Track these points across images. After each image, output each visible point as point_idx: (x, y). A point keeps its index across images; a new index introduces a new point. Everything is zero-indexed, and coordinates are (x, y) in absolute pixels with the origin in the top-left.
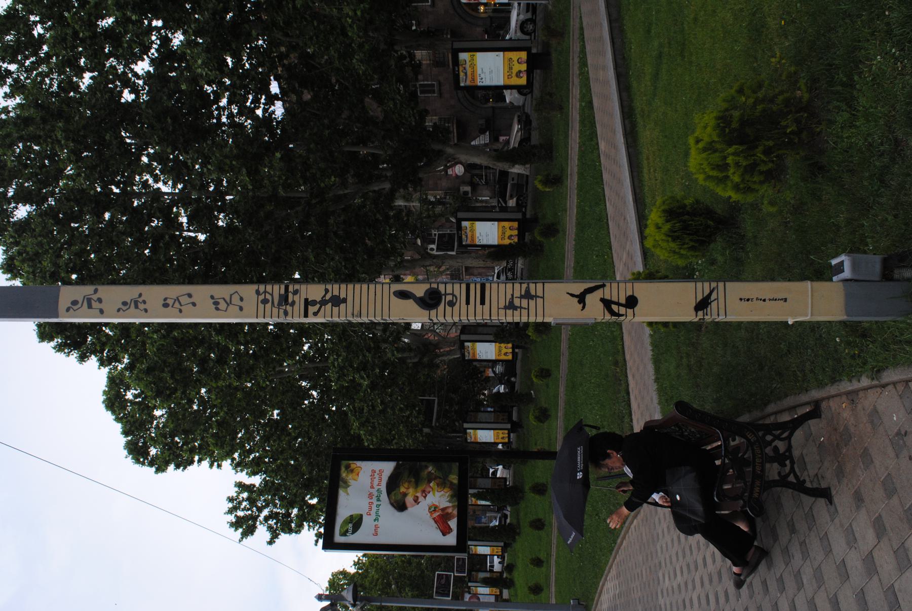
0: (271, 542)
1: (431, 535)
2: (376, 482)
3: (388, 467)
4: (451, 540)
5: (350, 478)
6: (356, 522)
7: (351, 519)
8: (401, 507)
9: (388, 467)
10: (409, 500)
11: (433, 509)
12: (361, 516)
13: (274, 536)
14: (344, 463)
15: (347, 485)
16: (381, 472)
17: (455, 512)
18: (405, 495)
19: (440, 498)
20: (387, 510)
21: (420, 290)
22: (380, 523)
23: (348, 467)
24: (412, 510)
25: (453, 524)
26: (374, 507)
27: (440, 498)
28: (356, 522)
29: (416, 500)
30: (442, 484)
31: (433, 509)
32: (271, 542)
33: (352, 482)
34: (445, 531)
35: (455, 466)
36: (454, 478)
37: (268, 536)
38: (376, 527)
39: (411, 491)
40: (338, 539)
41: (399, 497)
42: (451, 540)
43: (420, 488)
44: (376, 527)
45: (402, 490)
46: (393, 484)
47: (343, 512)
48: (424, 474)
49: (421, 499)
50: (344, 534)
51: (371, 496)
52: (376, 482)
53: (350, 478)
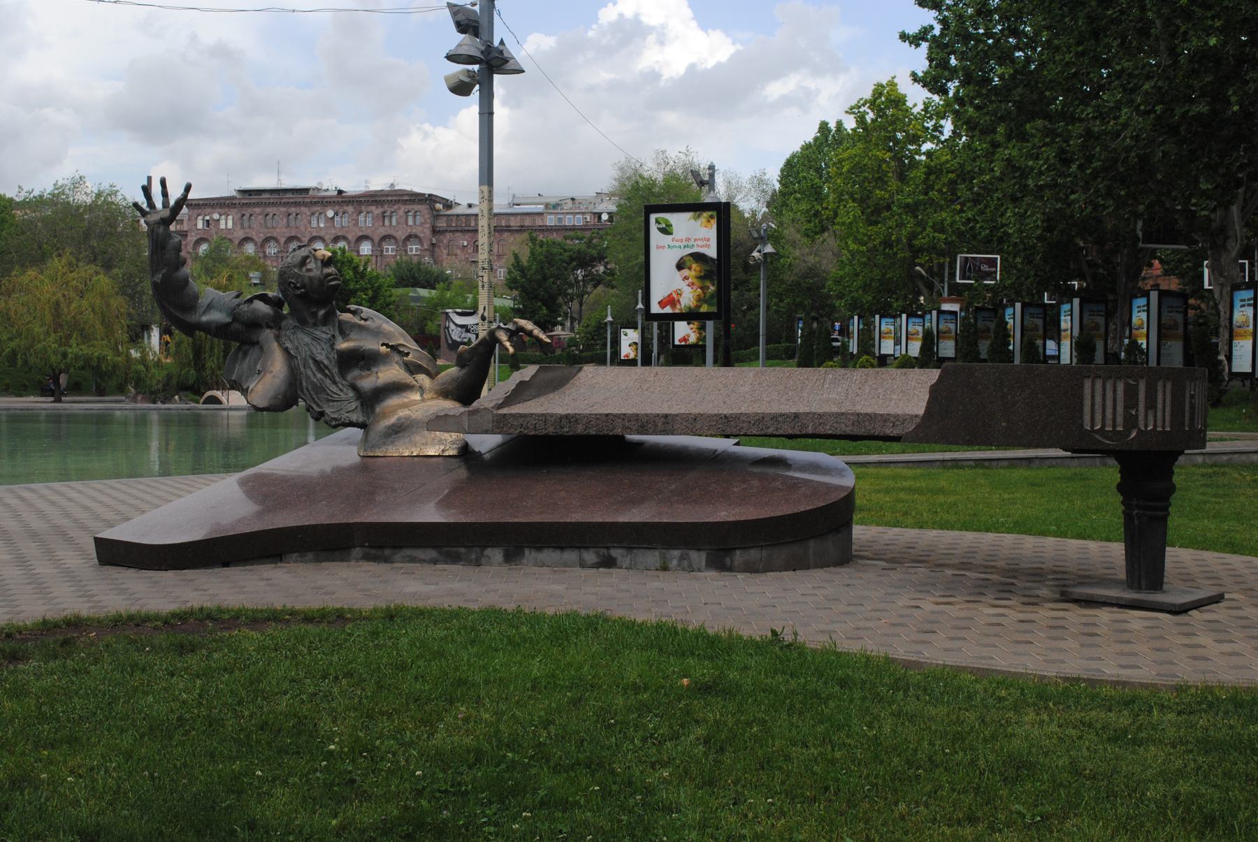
0: (904, 37)
1: (657, 294)
2: (700, 243)
3: (712, 252)
6: (666, 231)
7: (670, 226)
8: (680, 266)
9: (712, 252)
10: (686, 272)
12: (670, 234)
13: (914, 40)
14: (715, 213)
15: (696, 218)
16: (708, 246)
18: (690, 268)
20: (677, 255)
21: (486, 314)
22: (666, 249)
23: (711, 217)
24: (678, 275)
25: (668, 310)
26: (678, 244)
27: (688, 298)
29: (686, 278)
30: (700, 300)
32: (904, 37)
33: (699, 222)
34: (662, 304)
35: (714, 309)
37: (913, 30)
38: (663, 247)
39: (693, 273)
40: (653, 217)
41: (688, 264)
43: (695, 281)
44: (663, 247)
45: (694, 266)
46: (699, 257)
47: (675, 219)
48: (708, 283)
49: (687, 282)
50: (657, 221)
51: (688, 240)
52: (700, 243)
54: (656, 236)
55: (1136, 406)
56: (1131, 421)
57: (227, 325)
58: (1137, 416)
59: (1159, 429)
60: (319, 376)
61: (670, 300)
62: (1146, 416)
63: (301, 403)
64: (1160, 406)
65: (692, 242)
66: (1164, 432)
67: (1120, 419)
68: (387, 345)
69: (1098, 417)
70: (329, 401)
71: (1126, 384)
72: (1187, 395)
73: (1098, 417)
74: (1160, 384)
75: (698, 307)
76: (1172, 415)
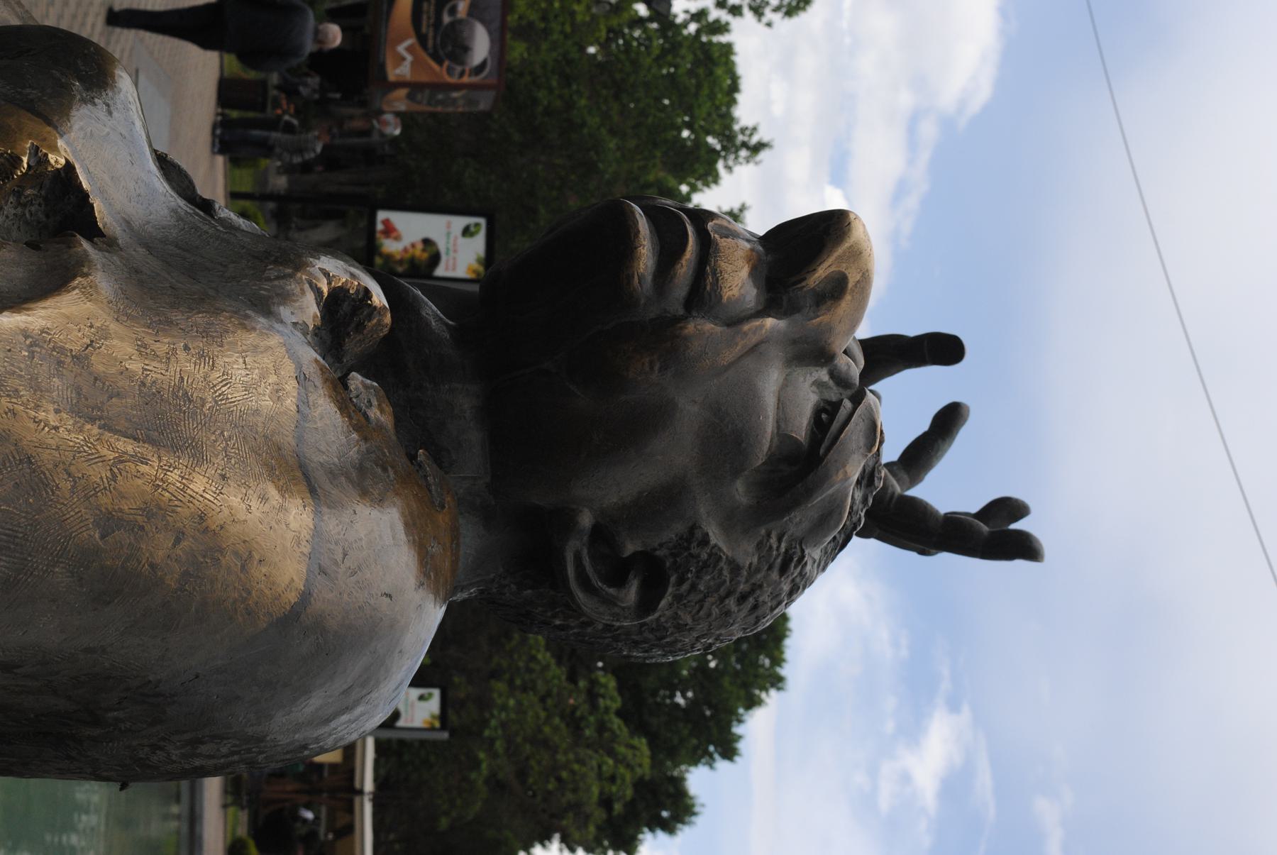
1: (400, 219)
2: (451, 262)
3: (440, 271)
4: (382, 215)
5: (476, 266)
6: (467, 232)
8: (427, 242)
9: (440, 271)
10: (420, 246)
11: (398, 238)
15: (479, 261)
16: (447, 269)
17: (378, 235)
18: (424, 250)
19: (391, 247)
25: (380, 227)
28: (467, 232)
30: (388, 258)
31: (398, 238)
34: (386, 222)
36: (378, 261)
42: (382, 215)
45: (425, 255)
46: (435, 259)
48: (406, 266)
50: (477, 225)
52: (451, 262)
53: (476, 266)
54: (460, 222)
61: (389, 230)
65: (451, 253)
75: (381, 255)
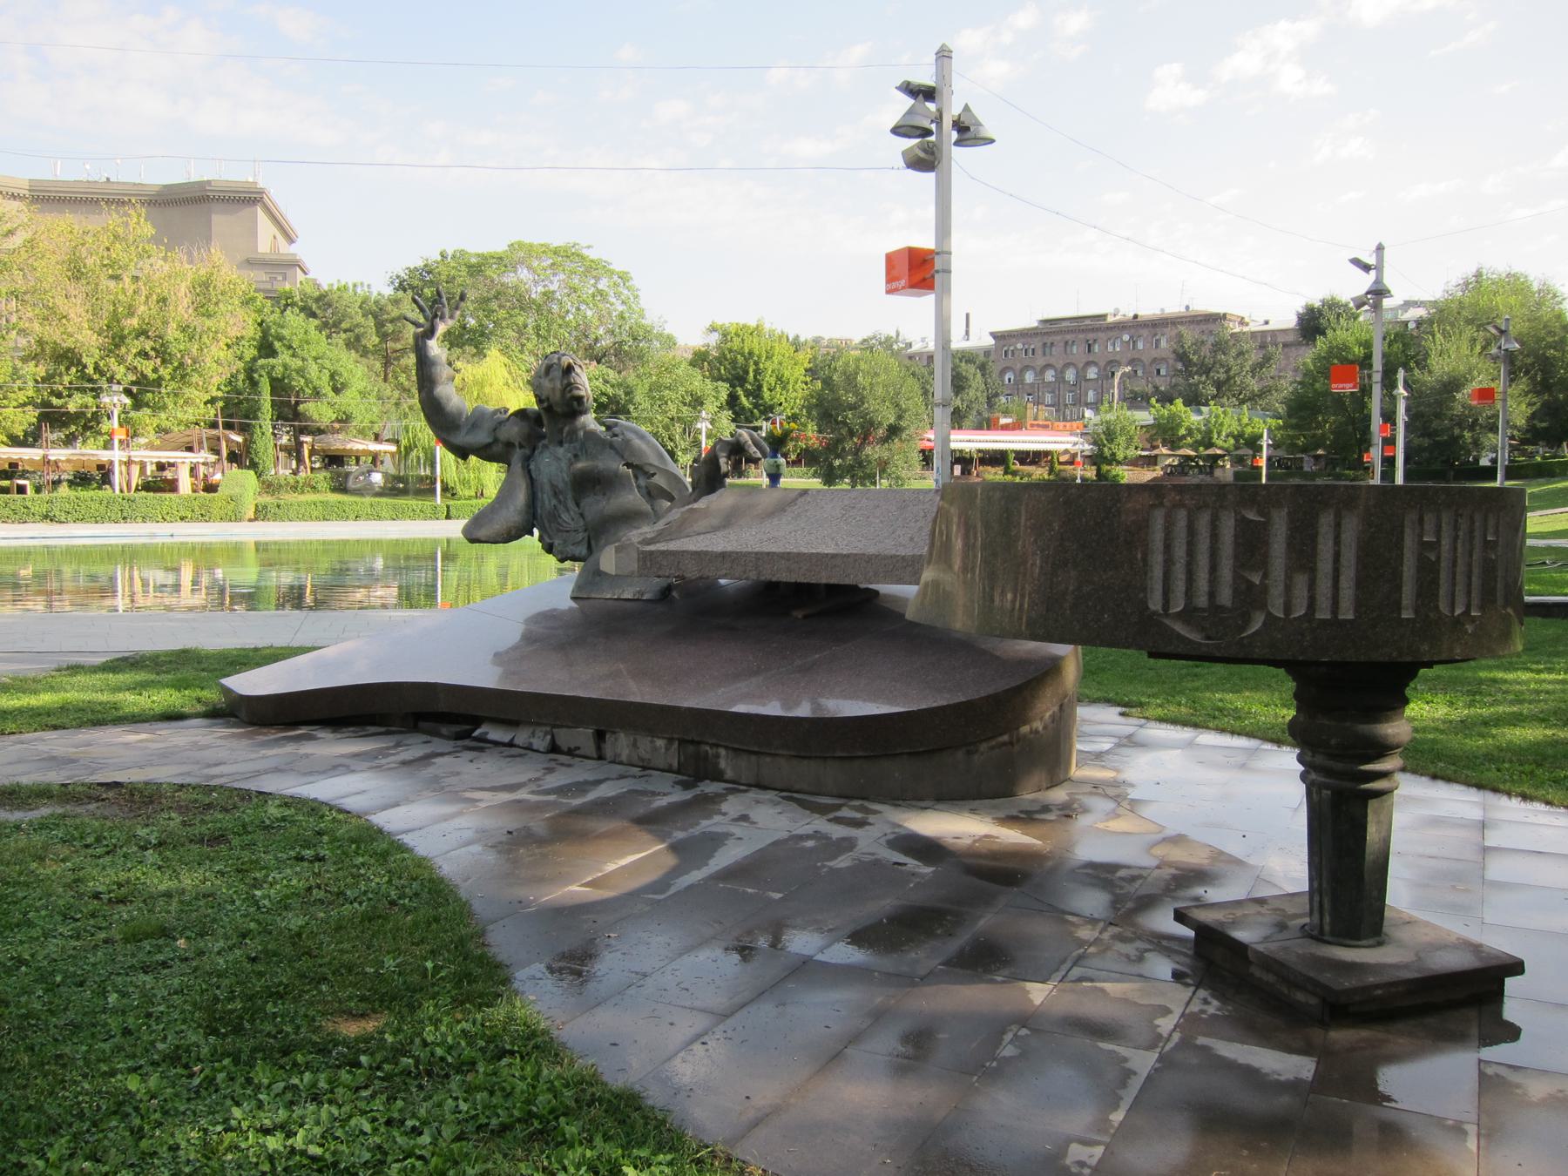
55: (1264, 565)
56: (1250, 597)
57: (488, 446)
58: (1264, 589)
59: (1323, 614)
60: (554, 502)
62: (1288, 589)
63: (536, 531)
64: (1325, 566)
66: (1335, 622)
67: (1225, 597)
68: (628, 465)
69: (1180, 586)
70: (559, 530)
71: (1243, 525)
72: (1409, 542)
73: (1180, 586)
74: (1326, 521)
76: (1360, 584)
